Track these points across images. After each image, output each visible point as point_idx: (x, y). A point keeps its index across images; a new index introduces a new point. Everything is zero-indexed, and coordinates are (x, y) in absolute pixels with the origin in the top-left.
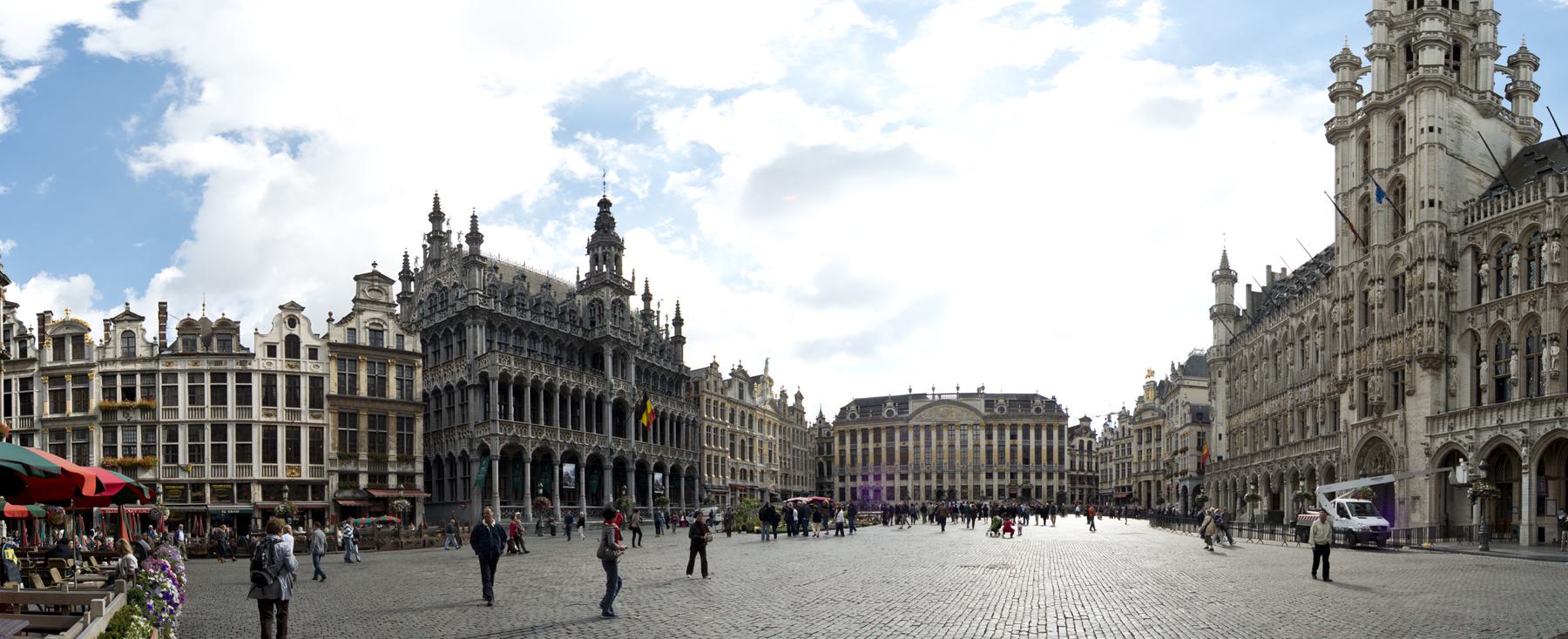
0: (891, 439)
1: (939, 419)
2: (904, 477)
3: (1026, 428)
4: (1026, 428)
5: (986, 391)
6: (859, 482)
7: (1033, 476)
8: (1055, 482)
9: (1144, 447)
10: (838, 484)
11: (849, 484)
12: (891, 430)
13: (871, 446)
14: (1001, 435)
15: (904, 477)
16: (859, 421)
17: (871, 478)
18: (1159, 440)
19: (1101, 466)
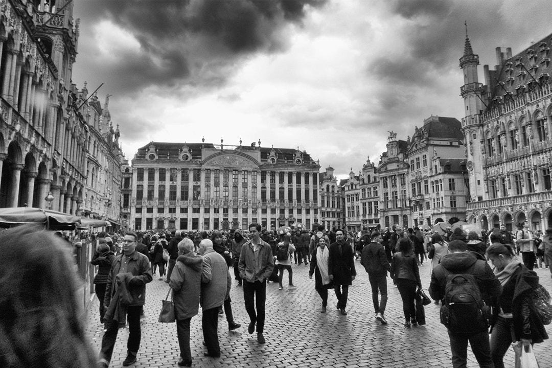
0: (185, 178)
1: (226, 165)
3: (290, 175)
4: (290, 175)
5: (262, 146)
7: (295, 211)
8: (311, 216)
9: (390, 190)
13: (168, 183)
14: (273, 181)
16: (157, 161)
17: (167, 210)
18: (403, 184)
19: (347, 204)
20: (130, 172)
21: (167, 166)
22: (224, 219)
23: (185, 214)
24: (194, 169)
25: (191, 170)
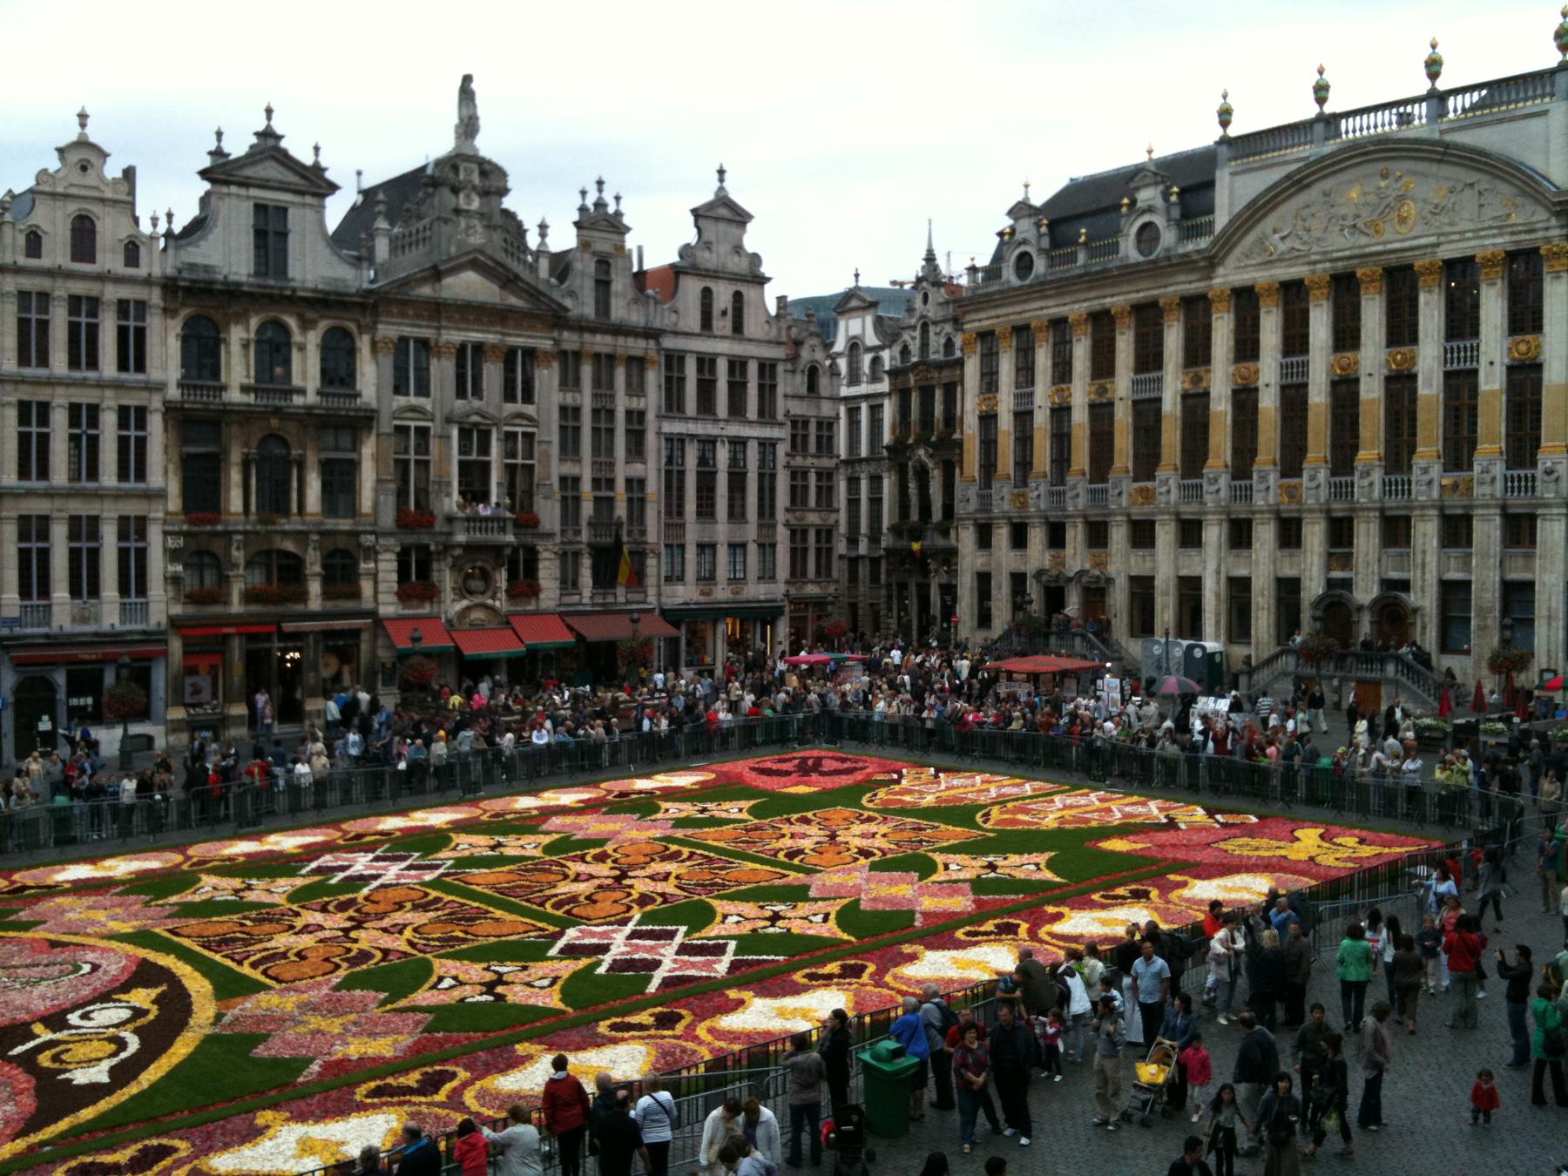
6: (1037, 554)
10: (970, 559)
11: (1004, 558)
12: (1148, 317)
13: (1080, 395)
16: (1042, 289)
17: (1075, 536)
20: (958, 354)
21: (1075, 308)
22: (1331, 583)
23: (1146, 552)
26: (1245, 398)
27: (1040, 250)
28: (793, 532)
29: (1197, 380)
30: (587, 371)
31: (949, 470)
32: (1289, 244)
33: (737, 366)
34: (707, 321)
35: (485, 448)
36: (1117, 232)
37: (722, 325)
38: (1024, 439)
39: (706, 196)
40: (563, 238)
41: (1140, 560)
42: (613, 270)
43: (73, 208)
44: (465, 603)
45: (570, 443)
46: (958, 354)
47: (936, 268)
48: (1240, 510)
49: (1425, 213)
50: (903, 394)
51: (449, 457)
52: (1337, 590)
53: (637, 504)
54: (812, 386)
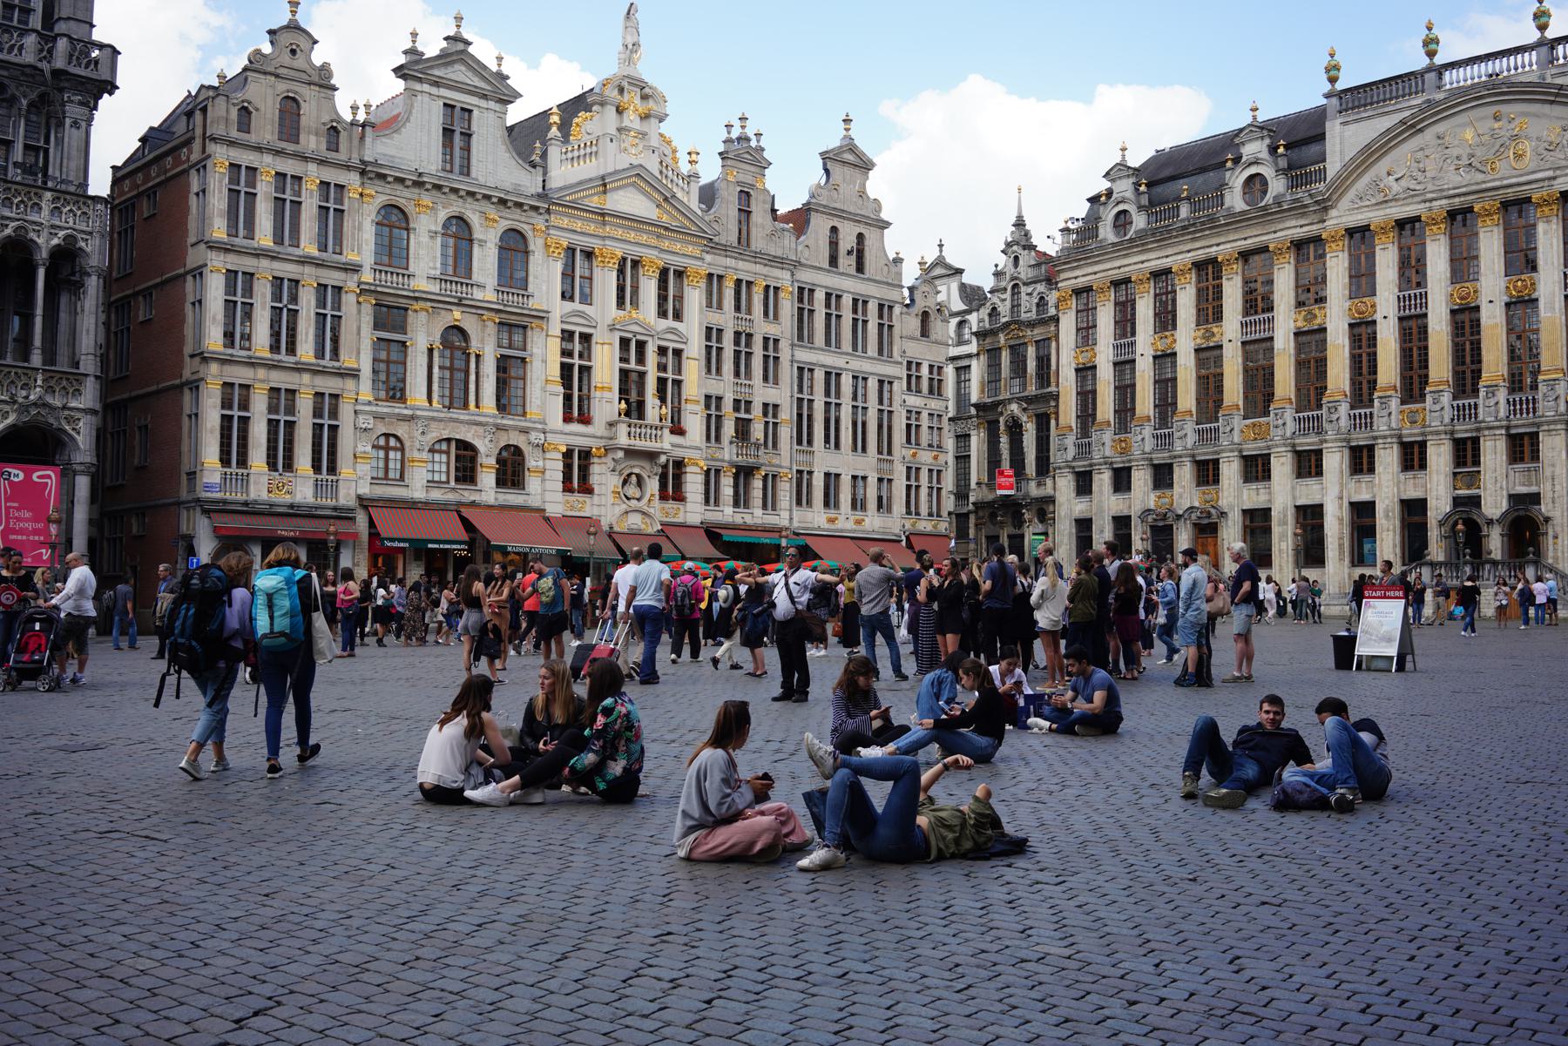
0: (1258, 303)
1: (1457, 180)
2: (1309, 464)
6: (1142, 494)
10: (1068, 505)
13: (1186, 339)
15: (1309, 464)
17: (1184, 475)
21: (1178, 257)
22: (1457, 501)
23: (1261, 485)
24: (1299, 245)
25: (1279, 252)
26: (1363, 333)
27: (1140, 208)
28: (909, 468)
29: (1311, 317)
30: (729, 294)
31: (1043, 422)
32: (1403, 183)
33: (859, 303)
34: (833, 261)
35: (641, 359)
36: (1223, 185)
37: (847, 263)
38: (1125, 392)
39: (834, 141)
40: (710, 170)
41: (1253, 493)
42: (753, 202)
43: (282, 87)
44: (624, 507)
45: (712, 360)
46: (1052, 311)
47: (1027, 235)
48: (1360, 438)
49: (1541, 150)
50: (993, 354)
51: (605, 365)
52: (1466, 505)
53: (772, 430)
54: (925, 333)
